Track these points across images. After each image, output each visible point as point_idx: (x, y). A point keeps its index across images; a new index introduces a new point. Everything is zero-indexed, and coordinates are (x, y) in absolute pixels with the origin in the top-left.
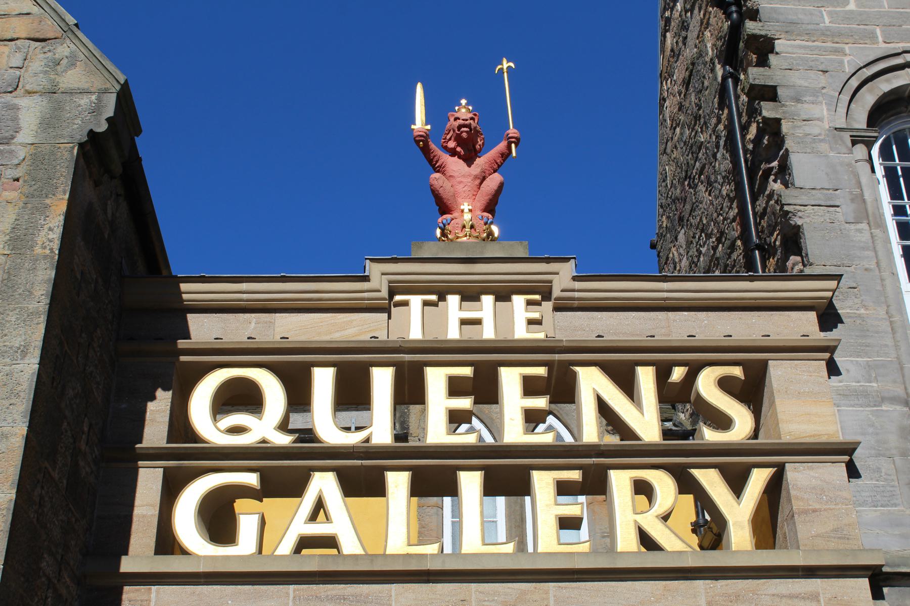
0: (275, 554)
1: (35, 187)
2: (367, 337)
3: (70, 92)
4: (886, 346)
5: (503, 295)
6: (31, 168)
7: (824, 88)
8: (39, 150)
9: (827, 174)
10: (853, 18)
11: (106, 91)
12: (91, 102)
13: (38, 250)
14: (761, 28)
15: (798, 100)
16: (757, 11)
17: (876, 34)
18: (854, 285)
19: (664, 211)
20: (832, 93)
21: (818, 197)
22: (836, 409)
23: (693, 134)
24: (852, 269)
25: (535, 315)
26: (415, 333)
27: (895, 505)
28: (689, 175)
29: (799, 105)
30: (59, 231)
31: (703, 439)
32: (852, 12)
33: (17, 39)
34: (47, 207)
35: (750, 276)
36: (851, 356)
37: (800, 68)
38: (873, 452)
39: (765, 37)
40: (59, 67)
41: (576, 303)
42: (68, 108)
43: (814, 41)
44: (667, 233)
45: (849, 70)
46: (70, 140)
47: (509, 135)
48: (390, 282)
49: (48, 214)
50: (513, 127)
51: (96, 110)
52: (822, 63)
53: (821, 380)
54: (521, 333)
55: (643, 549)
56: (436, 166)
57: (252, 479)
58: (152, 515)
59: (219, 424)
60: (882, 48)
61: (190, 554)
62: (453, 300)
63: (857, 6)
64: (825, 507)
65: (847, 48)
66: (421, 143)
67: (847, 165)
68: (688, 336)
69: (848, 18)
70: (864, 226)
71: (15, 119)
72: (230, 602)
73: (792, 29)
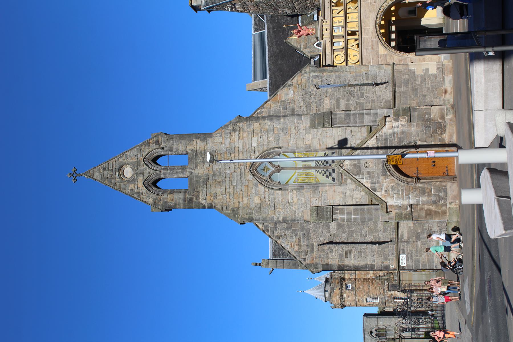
3: (310, 70)
11: (310, 66)
30: (330, 67)
34: (327, 69)
71: (314, 76)
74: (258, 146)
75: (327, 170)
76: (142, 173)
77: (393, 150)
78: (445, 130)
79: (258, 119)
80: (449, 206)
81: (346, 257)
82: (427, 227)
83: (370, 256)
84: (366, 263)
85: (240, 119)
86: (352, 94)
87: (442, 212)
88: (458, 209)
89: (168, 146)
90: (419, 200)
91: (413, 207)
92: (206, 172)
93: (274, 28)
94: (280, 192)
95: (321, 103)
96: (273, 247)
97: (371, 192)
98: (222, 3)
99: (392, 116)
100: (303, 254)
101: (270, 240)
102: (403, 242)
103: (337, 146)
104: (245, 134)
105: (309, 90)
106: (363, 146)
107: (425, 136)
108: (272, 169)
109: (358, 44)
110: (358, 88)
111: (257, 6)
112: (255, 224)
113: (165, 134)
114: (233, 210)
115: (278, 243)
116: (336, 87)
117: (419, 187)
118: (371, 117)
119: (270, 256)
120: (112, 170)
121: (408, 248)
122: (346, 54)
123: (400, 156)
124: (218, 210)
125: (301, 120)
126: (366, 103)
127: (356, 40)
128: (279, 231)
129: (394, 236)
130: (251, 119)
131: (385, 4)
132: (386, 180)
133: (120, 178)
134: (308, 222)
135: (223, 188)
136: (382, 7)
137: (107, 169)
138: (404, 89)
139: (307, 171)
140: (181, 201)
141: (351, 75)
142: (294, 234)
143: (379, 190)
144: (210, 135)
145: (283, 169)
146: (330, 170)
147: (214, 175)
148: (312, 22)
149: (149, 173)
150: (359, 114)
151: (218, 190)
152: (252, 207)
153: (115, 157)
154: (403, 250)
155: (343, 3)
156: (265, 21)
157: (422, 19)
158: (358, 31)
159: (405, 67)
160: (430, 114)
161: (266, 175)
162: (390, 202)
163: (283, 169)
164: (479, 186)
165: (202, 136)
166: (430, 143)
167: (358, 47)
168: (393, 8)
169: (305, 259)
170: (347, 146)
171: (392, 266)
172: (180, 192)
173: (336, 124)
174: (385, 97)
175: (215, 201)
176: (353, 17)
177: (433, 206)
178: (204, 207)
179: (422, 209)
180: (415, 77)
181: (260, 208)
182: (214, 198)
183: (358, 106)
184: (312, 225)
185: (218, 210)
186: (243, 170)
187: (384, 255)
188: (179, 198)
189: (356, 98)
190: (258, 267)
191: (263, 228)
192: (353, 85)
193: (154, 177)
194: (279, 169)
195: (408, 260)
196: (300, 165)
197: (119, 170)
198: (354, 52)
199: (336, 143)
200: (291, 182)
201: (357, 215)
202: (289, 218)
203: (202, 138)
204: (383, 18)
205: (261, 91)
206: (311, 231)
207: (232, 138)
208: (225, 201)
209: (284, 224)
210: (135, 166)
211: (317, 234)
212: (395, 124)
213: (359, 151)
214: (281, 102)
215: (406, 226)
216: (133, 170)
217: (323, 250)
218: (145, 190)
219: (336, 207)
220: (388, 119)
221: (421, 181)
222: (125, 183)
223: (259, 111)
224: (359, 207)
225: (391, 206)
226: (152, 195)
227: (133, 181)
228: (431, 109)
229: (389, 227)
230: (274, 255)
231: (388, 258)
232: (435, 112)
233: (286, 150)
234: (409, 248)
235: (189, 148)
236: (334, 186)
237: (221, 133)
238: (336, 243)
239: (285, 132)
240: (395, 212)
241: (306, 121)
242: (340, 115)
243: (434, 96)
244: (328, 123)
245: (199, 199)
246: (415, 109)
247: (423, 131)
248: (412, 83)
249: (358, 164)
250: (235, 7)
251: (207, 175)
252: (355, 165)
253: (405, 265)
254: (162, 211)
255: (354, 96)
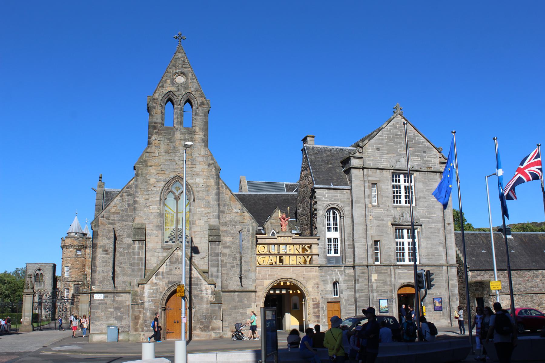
60: (329, 202)
74: (196, 183)
75: (174, 237)
76: (179, 90)
77: (188, 290)
78: (203, 331)
79: (218, 184)
80: (142, 333)
81: (104, 251)
82: (125, 316)
83: (103, 269)
84: (98, 266)
85: (218, 170)
86: (234, 259)
87: (137, 328)
88: (139, 341)
89: (199, 112)
90: (148, 310)
91: (142, 305)
92: (177, 141)
93: (288, 199)
94: (159, 199)
95: (228, 233)
96: (114, 192)
97: (155, 272)
98: (308, 160)
99: (216, 289)
100: (107, 215)
101: (120, 190)
102: (114, 297)
103: (193, 245)
104: (206, 173)
105: (239, 225)
106: (192, 266)
107: (198, 315)
108: (177, 194)
109: (272, 264)
110: (239, 263)
111: (305, 187)
112: (134, 178)
113: (209, 111)
114: (145, 161)
115: (117, 196)
116: (240, 246)
117: (158, 310)
118: (215, 273)
119: (106, 189)
120: (183, 67)
121: (109, 301)
122: (265, 255)
123: (183, 296)
124: (147, 149)
125: (215, 218)
126: (227, 269)
127: (276, 262)
128: (127, 197)
129: (119, 289)
130: (218, 178)
131: (302, 285)
132: (164, 284)
133: (175, 73)
134: (133, 221)
135: (164, 154)
136: (300, 283)
137: (183, 63)
138: (236, 299)
139: (174, 222)
140: (155, 120)
141: (249, 258)
142: (124, 209)
143: (157, 278)
144: (207, 146)
145: (177, 202)
146: (174, 240)
147: (174, 147)
148: (291, 229)
149: (178, 96)
150: (218, 264)
151: (162, 150)
152: (148, 176)
153: (192, 70)
154: (107, 296)
155: (304, 254)
156: (293, 193)
157: (290, 314)
158: (282, 264)
159: (253, 300)
160: (216, 319)
161: (173, 188)
162: (147, 287)
163: (177, 202)
164: (156, 357)
165: (206, 139)
166: (193, 319)
167: (270, 264)
168: (299, 292)
169: (103, 217)
170: (193, 254)
171: (94, 288)
172: (162, 120)
173: (211, 245)
174: (231, 284)
175: (154, 147)
176: (293, 261)
177: (142, 321)
178: (149, 138)
179: (140, 312)
180: (246, 308)
181: (146, 182)
182: (156, 146)
183: (224, 263)
184: (131, 224)
185: (147, 149)
186: (177, 171)
187: (103, 281)
188: (157, 118)
189: (231, 262)
190: (99, 179)
191: (130, 184)
192: (241, 259)
193: (175, 100)
194: (177, 199)
195: (99, 300)
196: (180, 216)
197: (182, 73)
198: (266, 261)
199: (196, 245)
200: (166, 208)
201: (137, 260)
202: (137, 205)
203: (204, 140)
204: (292, 284)
205: (240, 187)
206: (125, 223)
207: (203, 163)
208: (153, 155)
209: (132, 201)
210: (185, 86)
211: (123, 227)
212: (209, 292)
213: (189, 263)
214: (230, 202)
215: (127, 299)
216: (182, 83)
217: (109, 232)
218: (165, 92)
219: (144, 243)
220: (213, 286)
221: (163, 312)
222: (171, 77)
223: (224, 185)
224: (144, 262)
225: (144, 287)
226: (161, 97)
227: (173, 83)
228: (220, 320)
229: (127, 286)
230: (107, 192)
231: (101, 285)
232: (218, 323)
233: (192, 205)
234: (108, 301)
235: (197, 129)
236: (162, 243)
237: (207, 155)
238: (115, 243)
239: (207, 205)
240: (138, 290)
241: (214, 221)
242: (218, 249)
243: (230, 323)
244: (211, 240)
245: (155, 134)
246: (220, 307)
247: (203, 314)
248: (240, 306)
249: (179, 262)
250: (305, 170)
251: (175, 141)
252: (178, 259)
253: (95, 298)
254: (147, 104)
255: (233, 260)
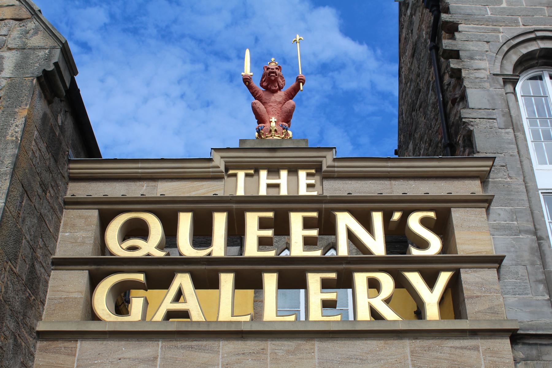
0: (152, 320)
1: (10, 102)
2: (211, 194)
3: (34, 49)
4: (523, 200)
5: (293, 170)
6: (8, 91)
7: (487, 51)
8: (13, 81)
9: (488, 100)
10: (505, 12)
11: (54, 48)
12: (45, 54)
13: (9, 138)
14: (450, 18)
15: (472, 58)
16: (448, 8)
17: (518, 20)
18: (504, 164)
19: (402, 132)
20: (492, 54)
21: (483, 114)
22: (492, 237)
23: (416, 85)
24: (503, 155)
25: (312, 181)
26: (240, 192)
27: (527, 294)
28: (414, 109)
29: (472, 61)
31: (410, 254)
32: (504, 8)
33: (6, 19)
34: (16, 113)
35: (440, 158)
36: (501, 206)
37: (473, 40)
38: (514, 262)
39: (452, 22)
40: (28, 35)
41: (336, 175)
42: (32, 57)
43: (482, 25)
44: (403, 145)
45: (502, 41)
46: (32, 75)
47: (299, 78)
48: (226, 162)
49: (16, 117)
50: (302, 73)
51: (48, 58)
52: (486, 37)
53: (483, 219)
54: (303, 191)
55: (373, 319)
56: (256, 96)
57: (141, 277)
58: (80, 298)
59: (122, 245)
60: (522, 29)
61: (101, 320)
62: (263, 173)
63: (507, 5)
64: (484, 294)
65: (501, 29)
66: (247, 83)
67: (500, 95)
68: (402, 194)
69: (502, 12)
70: (511, 130)
72: (123, 349)
73: (469, 18)
